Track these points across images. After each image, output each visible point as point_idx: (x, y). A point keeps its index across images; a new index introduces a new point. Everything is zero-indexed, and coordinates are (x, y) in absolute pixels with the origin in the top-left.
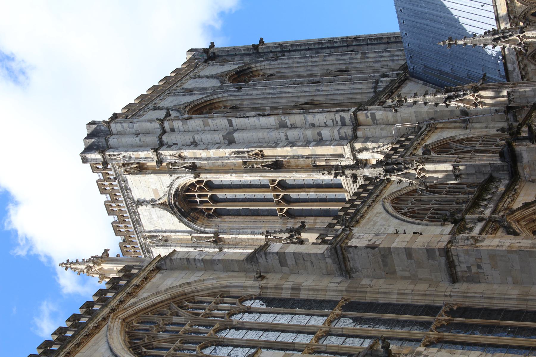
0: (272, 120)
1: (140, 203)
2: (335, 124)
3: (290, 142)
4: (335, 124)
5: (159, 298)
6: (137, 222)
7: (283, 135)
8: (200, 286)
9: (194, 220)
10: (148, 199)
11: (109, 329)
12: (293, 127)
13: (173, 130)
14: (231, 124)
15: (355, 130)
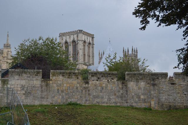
0: (82, 54)
1: (74, 36)
9: (72, 42)
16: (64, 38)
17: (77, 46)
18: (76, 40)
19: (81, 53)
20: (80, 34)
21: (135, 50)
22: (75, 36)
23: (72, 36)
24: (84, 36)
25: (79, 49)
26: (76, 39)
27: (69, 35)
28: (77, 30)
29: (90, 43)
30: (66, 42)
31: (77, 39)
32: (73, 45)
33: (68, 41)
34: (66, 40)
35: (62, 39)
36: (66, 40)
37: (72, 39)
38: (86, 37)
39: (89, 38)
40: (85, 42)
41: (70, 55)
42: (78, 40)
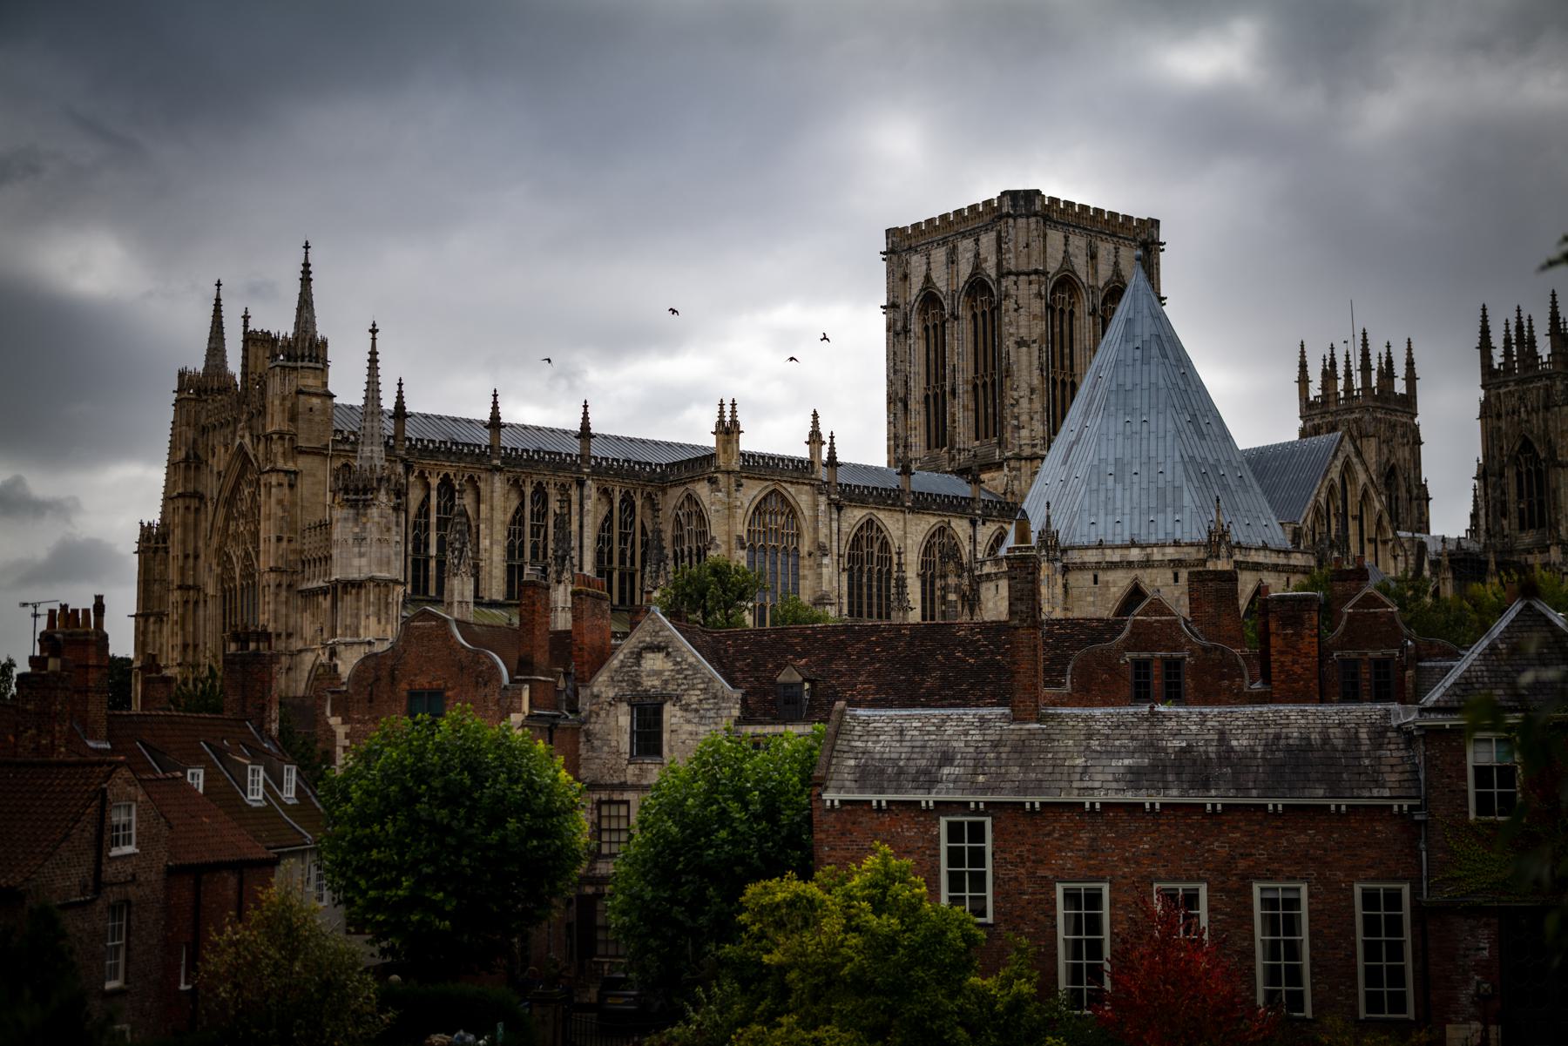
0: (1036, 382)
1: (977, 241)
2: (1033, 439)
3: (1017, 401)
4: (1033, 439)
5: (791, 500)
6: (964, 235)
7: (1022, 394)
8: (802, 520)
9: (968, 294)
10: (981, 251)
11: (767, 487)
12: (1031, 400)
13: (1030, 283)
14: (1034, 342)
15: (1026, 459)
16: (917, 262)
17: (1000, 319)
18: (993, 275)
19: (1026, 369)
20: (1022, 222)
22: (988, 241)
23: (966, 246)
24: (1055, 237)
25: (1010, 343)
26: (990, 268)
27: (945, 241)
28: (995, 194)
30: (930, 299)
31: (999, 264)
32: (974, 316)
33: (941, 284)
34: (928, 278)
35: (905, 277)
36: (928, 278)
37: (965, 270)
38: (1078, 243)
39: (1105, 249)
40: (1066, 282)
41: (953, 393)
42: (1002, 274)
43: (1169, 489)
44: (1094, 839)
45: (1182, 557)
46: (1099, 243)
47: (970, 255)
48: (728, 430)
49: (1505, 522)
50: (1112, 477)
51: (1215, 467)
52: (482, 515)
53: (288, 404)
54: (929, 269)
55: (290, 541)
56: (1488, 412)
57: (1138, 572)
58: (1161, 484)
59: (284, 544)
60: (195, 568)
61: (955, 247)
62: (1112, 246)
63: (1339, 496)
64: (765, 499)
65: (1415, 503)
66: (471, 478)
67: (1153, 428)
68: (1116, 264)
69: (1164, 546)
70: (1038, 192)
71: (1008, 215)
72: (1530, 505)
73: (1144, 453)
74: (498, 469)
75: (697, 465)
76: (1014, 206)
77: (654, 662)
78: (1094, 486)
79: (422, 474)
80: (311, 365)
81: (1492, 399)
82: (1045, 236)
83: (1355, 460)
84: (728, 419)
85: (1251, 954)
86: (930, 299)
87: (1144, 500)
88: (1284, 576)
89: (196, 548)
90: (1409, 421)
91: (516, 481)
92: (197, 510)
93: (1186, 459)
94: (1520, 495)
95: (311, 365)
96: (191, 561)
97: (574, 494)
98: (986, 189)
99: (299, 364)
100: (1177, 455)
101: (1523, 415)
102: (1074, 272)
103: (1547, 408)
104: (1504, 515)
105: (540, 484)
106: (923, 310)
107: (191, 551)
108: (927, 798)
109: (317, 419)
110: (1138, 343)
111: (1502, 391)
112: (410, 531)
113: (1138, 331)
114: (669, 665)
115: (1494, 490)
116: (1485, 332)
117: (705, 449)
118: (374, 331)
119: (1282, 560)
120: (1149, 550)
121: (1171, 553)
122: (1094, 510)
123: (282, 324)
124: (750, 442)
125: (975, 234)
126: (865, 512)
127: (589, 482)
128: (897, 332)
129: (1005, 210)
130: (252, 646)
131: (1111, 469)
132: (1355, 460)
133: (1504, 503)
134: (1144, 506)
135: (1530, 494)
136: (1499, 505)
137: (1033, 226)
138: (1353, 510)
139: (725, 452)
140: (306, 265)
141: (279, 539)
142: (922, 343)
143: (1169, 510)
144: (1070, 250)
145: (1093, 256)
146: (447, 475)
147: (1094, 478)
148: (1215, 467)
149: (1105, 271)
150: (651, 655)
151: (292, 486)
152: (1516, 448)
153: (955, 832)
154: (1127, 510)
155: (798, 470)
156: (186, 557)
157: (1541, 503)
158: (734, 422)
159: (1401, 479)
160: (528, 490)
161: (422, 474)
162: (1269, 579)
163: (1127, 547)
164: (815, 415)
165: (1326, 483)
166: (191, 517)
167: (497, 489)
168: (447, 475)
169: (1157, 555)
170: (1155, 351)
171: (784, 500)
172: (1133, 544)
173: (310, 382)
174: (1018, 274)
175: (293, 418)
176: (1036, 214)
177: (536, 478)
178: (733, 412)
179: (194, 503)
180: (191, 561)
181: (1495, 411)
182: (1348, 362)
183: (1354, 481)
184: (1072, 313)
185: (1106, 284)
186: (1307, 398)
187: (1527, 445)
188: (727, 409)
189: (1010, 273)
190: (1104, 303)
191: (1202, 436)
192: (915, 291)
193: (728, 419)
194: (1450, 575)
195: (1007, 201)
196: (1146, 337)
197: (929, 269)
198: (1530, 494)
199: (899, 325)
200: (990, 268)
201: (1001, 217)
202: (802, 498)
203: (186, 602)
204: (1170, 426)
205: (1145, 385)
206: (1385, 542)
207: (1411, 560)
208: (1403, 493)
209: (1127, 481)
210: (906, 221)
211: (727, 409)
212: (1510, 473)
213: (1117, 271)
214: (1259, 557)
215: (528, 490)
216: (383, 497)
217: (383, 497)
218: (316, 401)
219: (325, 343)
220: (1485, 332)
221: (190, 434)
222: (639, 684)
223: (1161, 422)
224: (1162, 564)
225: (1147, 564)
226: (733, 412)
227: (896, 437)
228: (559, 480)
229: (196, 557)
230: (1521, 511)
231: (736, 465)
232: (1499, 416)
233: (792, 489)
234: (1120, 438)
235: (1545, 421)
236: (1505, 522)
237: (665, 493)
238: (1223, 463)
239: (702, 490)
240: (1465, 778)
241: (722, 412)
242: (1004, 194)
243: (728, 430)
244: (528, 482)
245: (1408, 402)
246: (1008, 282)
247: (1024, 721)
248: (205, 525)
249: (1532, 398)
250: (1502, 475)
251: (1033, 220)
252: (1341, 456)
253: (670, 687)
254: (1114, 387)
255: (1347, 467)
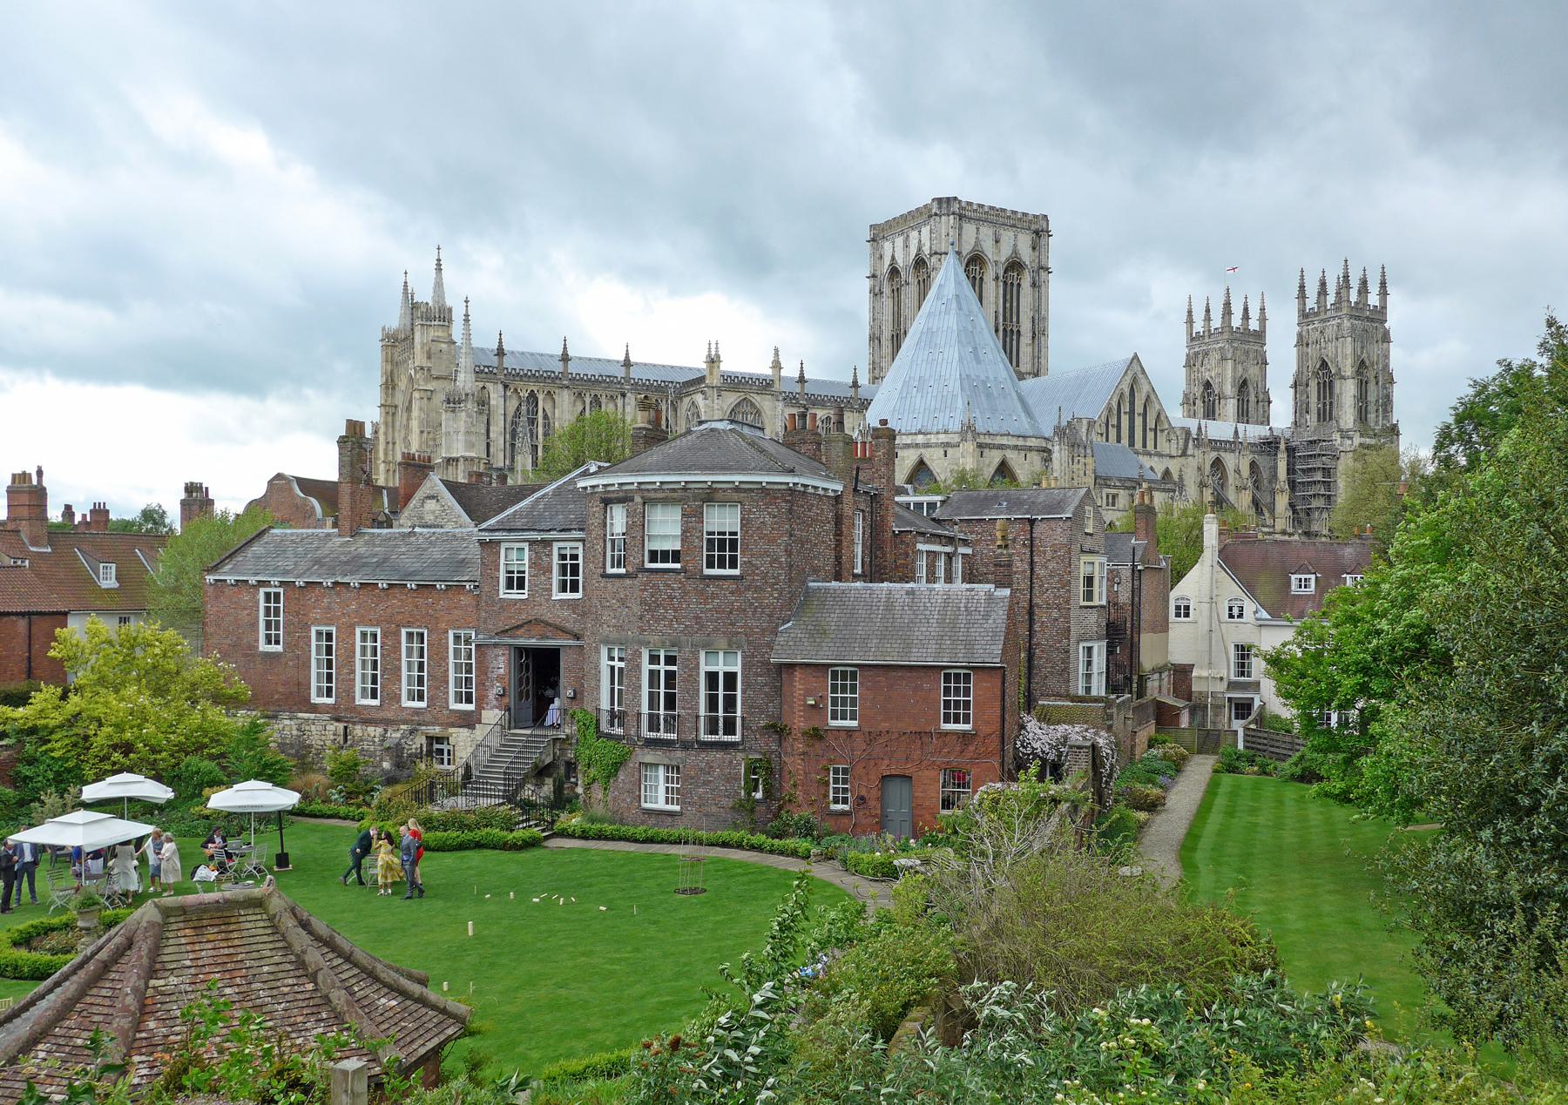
1: (920, 232)
6: (912, 228)
9: (915, 268)
16: (887, 245)
18: (927, 252)
21: (1364, 283)
24: (969, 229)
26: (926, 249)
29: (1015, 265)
30: (894, 272)
33: (900, 262)
34: (893, 258)
36: (893, 258)
37: (913, 251)
38: (987, 232)
39: (1007, 236)
43: (950, 396)
44: (330, 603)
45: (949, 441)
46: (1002, 232)
47: (916, 241)
48: (713, 361)
49: (1308, 417)
50: (915, 389)
51: (984, 382)
52: (557, 415)
53: (426, 348)
54: (894, 251)
55: (429, 433)
56: (1302, 342)
57: (923, 450)
58: (945, 393)
59: (425, 435)
60: (393, 450)
61: (908, 236)
62: (1011, 234)
63: (1127, 400)
64: (739, 403)
65: (1260, 404)
66: (549, 392)
67: (946, 357)
68: (1015, 246)
69: (938, 433)
70: (955, 198)
71: (936, 214)
72: (1325, 404)
73: (938, 374)
74: (567, 387)
75: (696, 382)
76: (940, 208)
77: (431, 505)
78: (904, 395)
79: (516, 390)
80: (441, 323)
81: (1304, 333)
82: (960, 228)
83: (1141, 376)
84: (713, 353)
85: (399, 669)
86: (894, 272)
87: (933, 403)
88: (1023, 453)
89: (393, 438)
90: (1260, 349)
91: (580, 394)
92: (394, 414)
93: (964, 376)
94: (1319, 400)
95: (441, 323)
96: (391, 445)
97: (620, 401)
98: (923, 198)
99: (433, 323)
100: (958, 373)
101: (1323, 345)
102: (983, 252)
103: (1337, 339)
104: (1307, 412)
105: (596, 395)
106: (891, 279)
107: (390, 439)
108: (253, 580)
109: (445, 357)
110: (944, 301)
111: (1310, 327)
112: (507, 426)
113: (946, 293)
114: (438, 507)
115: (1301, 395)
116: (1302, 287)
117: (699, 370)
118: (467, 302)
119: (1020, 442)
120: (929, 436)
121: (943, 438)
122: (902, 411)
123: (424, 295)
124: (728, 366)
125: (918, 228)
126: (825, 412)
127: (629, 395)
128: (876, 294)
129: (934, 211)
130: (194, 494)
131: (916, 384)
132: (1141, 376)
133: (1308, 404)
134: (933, 407)
135: (1325, 398)
136: (1304, 406)
137: (952, 221)
138: (1139, 409)
139: (711, 374)
140: (439, 260)
141: (422, 432)
142: (890, 300)
143: (948, 410)
144: (981, 237)
145: (997, 242)
146: (532, 391)
147: (905, 389)
148: (984, 382)
149: (1005, 253)
150: (429, 501)
151: (429, 399)
152: (1318, 367)
153: (268, 595)
154: (922, 411)
155: (765, 385)
156: (388, 443)
157: (1331, 403)
158: (718, 356)
159: (1251, 389)
160: (588, 400)
161: (516, 390)
162: (1011, 456)
163: (915, 434)
164: (776, 350)
165: (1117, 392)
166: (390, 419)
167: (565, 398)
168: (532, 391)
169: (933, 439)
170: (954, 305)
171: (752, 404)
172: (920, 432)
173: (440, 334)
174: (941, 254)
175: (429, 357)
176: (953, 214)
177: (593, 393)
178: (717, 348)
179: (391, 410)
180: (391, 445)
181: (1305, 341)
182: (1246, 310)
183: (1140, 391)
184: (981, 279)
185: (1007, 260)
186: (1191, 334)
187: (1324, 365)
188: (713, 346)
189: (936, 253)
190: (1005, 273)
191: (978, 361)
192: (886, 266)
193: (713, 353)
194: (1285, 456)
195: (935, 204)
196: (950, 297)
197: (894, 251)
198: (1325, 398)
199: (877, 288)
200: (926, 249)
201: (931, 216)
202: (765, 403)
203: (388, 470)
204: (956, 355)
205: (945, 328)
206: (1162, 431)
207: (1181, 442)
208: (1252, 398)
209: (925, 392)
210: (881, 221)
211: (713, 346)
212: (1313, 384)
213: (1015, 251)
214: (1004, 441)
215: (588, 400)
216: (469, 405)
217: (469, 405)
218: (443, 345)
219: (450, 310)
220: (1302, 287)
221: (389, 368)
222: (422, 518)
223: (951, 352)
224: (937, 445)
225: (927, 445)
226: (717, 348)
227: (873, 362)
228: (609, 394)
229: (394, 443)
230: (1319, 409)
231: (716, 382)
232: (1308, 345)
233: (758, 398)
234: (924, 363)
235: (1336, 348)
236: (1308, 417)
237: (682, 401)
238: (992, 378)
239: (699, 398)
240: (498, 570)
241: (710, 349)
242: (933, 200)
243: (713, 361)
244: (588, 395)
245: (1260, 336)
246: (934, 259)
247: (343, 536)
248: (398, 424)
249: (1330, 332)
250: (1307, 385)
251: (952, 217)
252: (1130, 374)
253: (438, 520)
254: (925, 330)
255: (1135, 379)
